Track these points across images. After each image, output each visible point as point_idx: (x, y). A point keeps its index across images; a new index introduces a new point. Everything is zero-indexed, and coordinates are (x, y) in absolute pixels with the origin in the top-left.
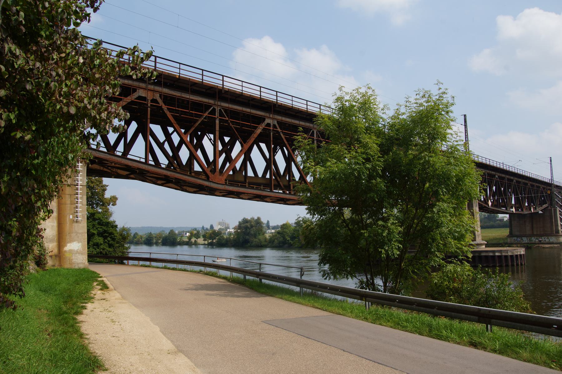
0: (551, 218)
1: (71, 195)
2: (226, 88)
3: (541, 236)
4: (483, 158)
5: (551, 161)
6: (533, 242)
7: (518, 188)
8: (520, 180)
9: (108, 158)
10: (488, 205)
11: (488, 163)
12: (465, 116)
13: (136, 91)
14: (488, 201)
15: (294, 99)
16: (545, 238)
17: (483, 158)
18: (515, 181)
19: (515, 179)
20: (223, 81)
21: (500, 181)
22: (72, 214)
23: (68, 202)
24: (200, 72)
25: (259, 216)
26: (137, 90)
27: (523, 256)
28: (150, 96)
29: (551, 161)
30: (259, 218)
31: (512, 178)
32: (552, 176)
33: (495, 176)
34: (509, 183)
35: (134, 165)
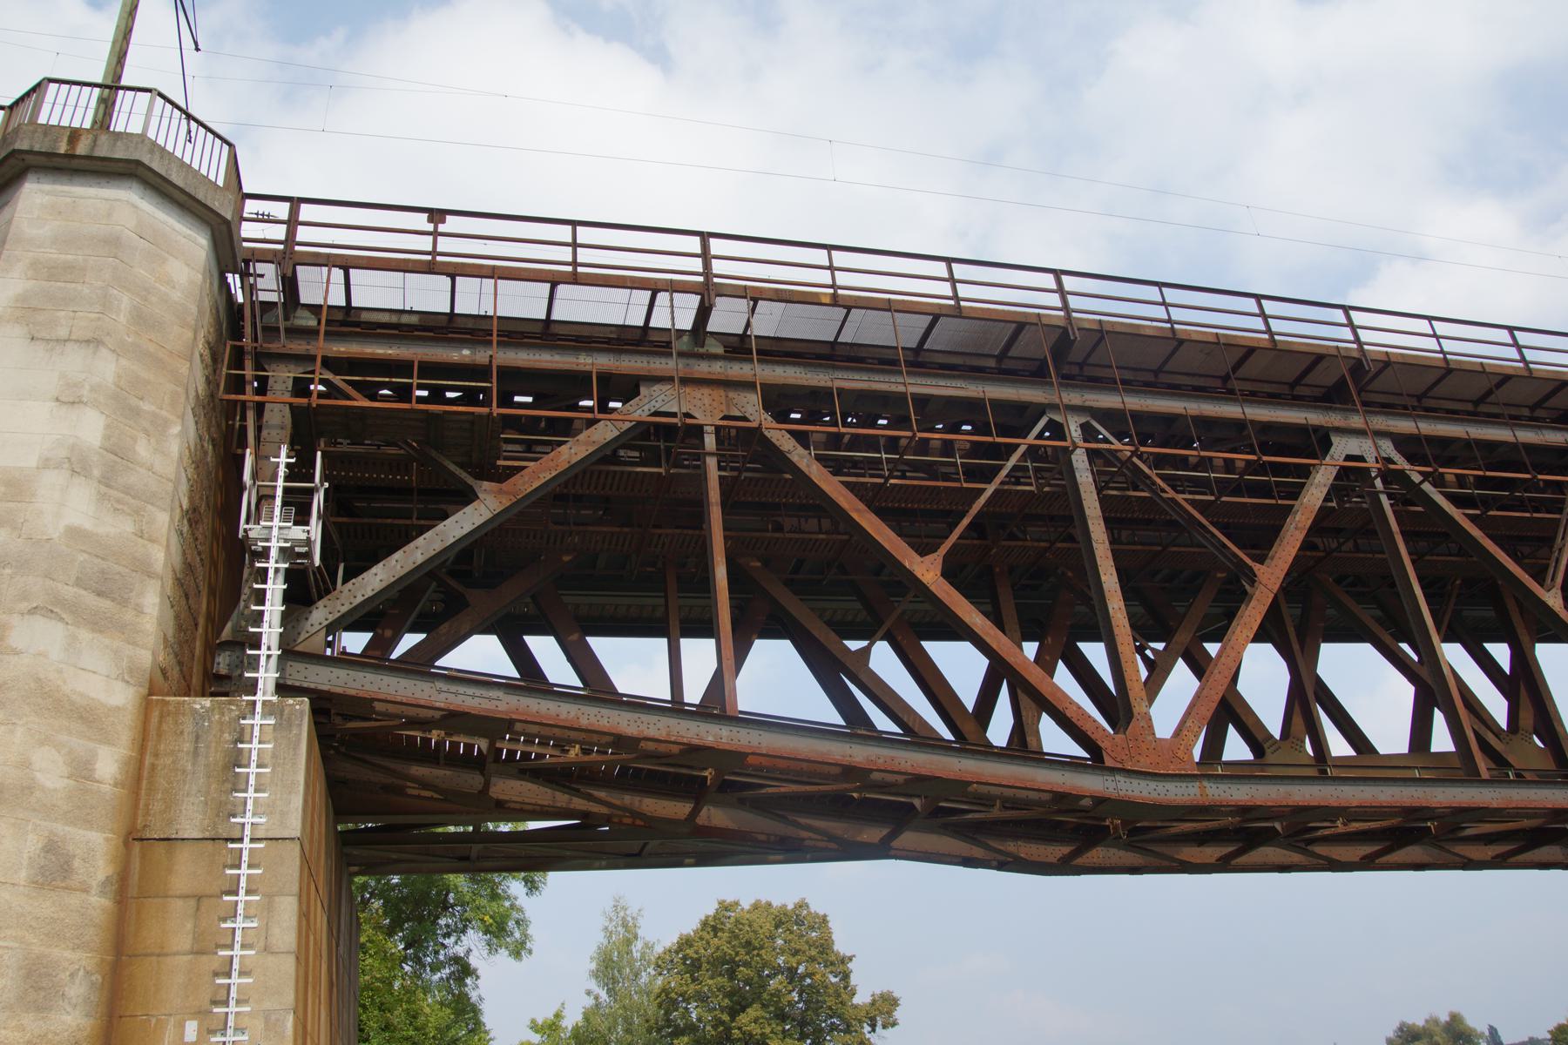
1: (199, 898)
2: (1088, 320)
9: (502, 707)
13: (638, 394)
15: (1441, 328)
20: (1060, 290)
22: (201, 1014)
23: (181, 940)
24: (940, 269)
25: (1455, 1009)
26: (643, 390)
28: (705, 409)
30: (1455, 1018)
35: (652, 732)
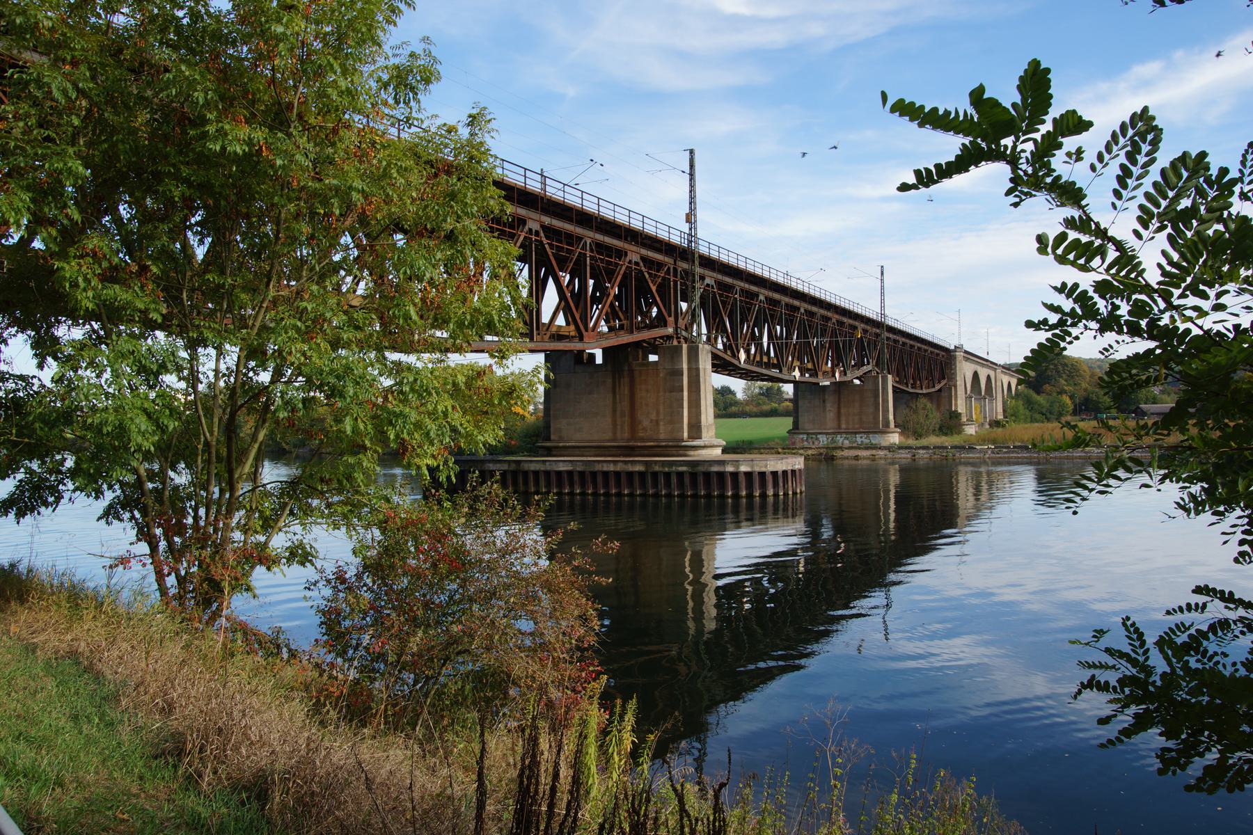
0: (877, 396)
4: (730, 254)
5: (882, 274)
6: (840, 444)
7: (810, 326)
8: (814, 309)
10: (739, 359)
11: (742, 265)
12: (692, 152)
14: (738, 352)
17: (730, 254)
18: (802, 310)
19: (804, 306)
21: (769, 309)
27: (797, 473)
29: (882, 274)
31: (796, 303)
32: (883, 307)
33: (758, 296)
34: (789, 315)
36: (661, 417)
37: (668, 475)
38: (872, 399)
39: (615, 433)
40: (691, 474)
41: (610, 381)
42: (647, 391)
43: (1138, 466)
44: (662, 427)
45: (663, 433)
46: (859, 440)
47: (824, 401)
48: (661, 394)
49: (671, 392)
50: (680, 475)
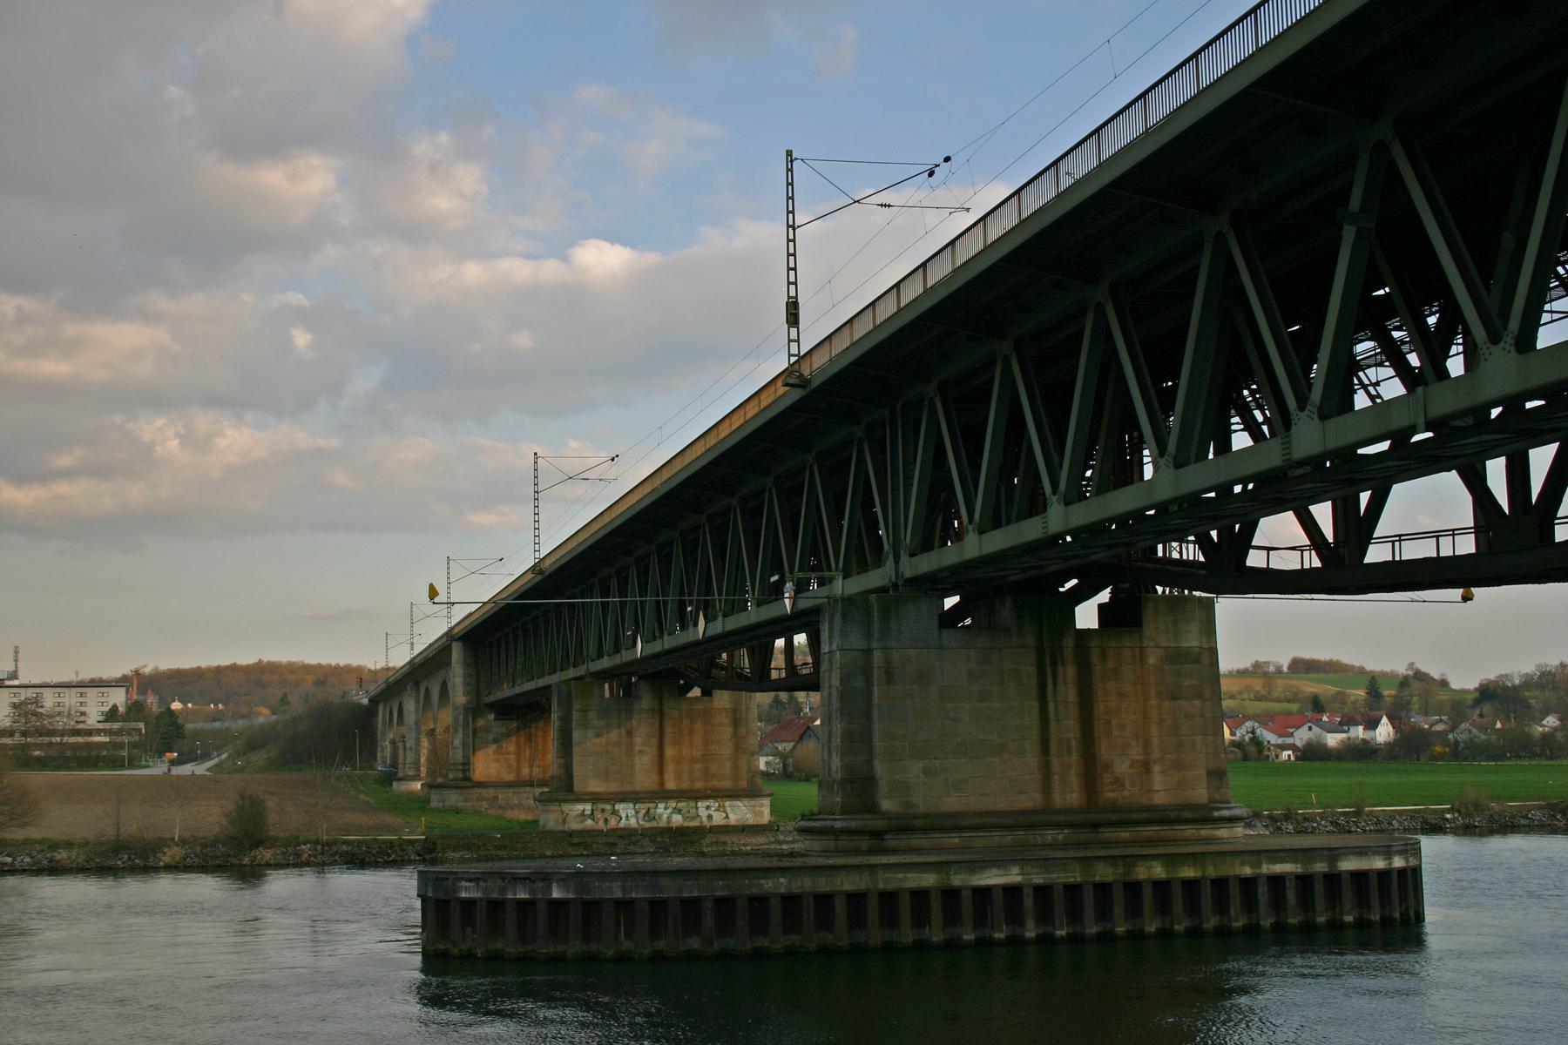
3: (695, 796)
16: (708, 808)
36: (1156, 754)
37: (1249, 884)
38: (730, 730)
39: (1047, 789)
40: (1299, 877)
41: (1030, 669)
42: (1121, 695)
43: (334, 863)
44: (1158, 781)
45: (1161, 791)
46: (703, 813)
47: (630, 733)
48: (1153, 702)
49: (1175, 697)
50: (1276, 881)
